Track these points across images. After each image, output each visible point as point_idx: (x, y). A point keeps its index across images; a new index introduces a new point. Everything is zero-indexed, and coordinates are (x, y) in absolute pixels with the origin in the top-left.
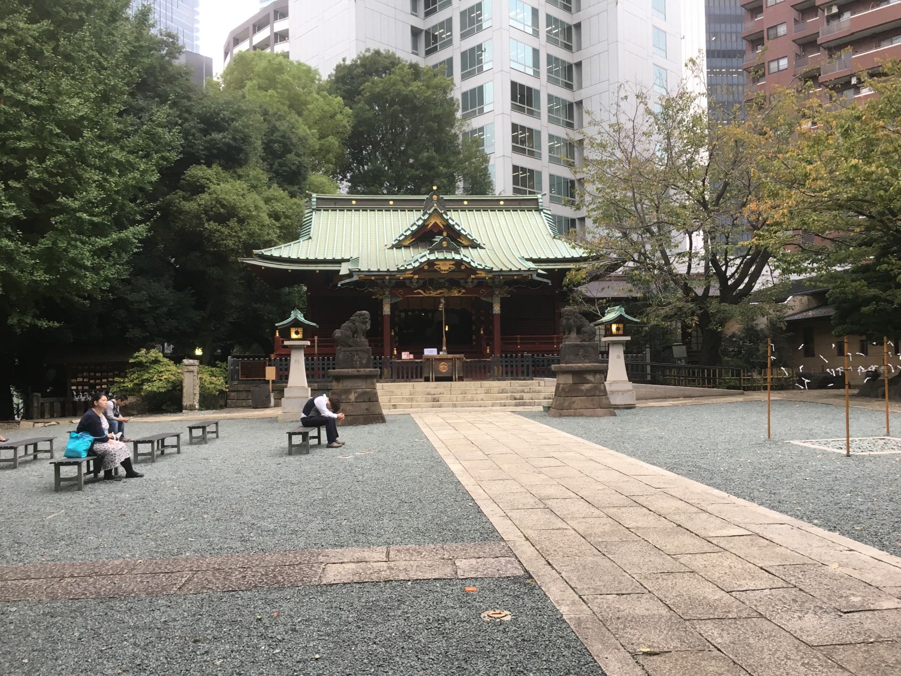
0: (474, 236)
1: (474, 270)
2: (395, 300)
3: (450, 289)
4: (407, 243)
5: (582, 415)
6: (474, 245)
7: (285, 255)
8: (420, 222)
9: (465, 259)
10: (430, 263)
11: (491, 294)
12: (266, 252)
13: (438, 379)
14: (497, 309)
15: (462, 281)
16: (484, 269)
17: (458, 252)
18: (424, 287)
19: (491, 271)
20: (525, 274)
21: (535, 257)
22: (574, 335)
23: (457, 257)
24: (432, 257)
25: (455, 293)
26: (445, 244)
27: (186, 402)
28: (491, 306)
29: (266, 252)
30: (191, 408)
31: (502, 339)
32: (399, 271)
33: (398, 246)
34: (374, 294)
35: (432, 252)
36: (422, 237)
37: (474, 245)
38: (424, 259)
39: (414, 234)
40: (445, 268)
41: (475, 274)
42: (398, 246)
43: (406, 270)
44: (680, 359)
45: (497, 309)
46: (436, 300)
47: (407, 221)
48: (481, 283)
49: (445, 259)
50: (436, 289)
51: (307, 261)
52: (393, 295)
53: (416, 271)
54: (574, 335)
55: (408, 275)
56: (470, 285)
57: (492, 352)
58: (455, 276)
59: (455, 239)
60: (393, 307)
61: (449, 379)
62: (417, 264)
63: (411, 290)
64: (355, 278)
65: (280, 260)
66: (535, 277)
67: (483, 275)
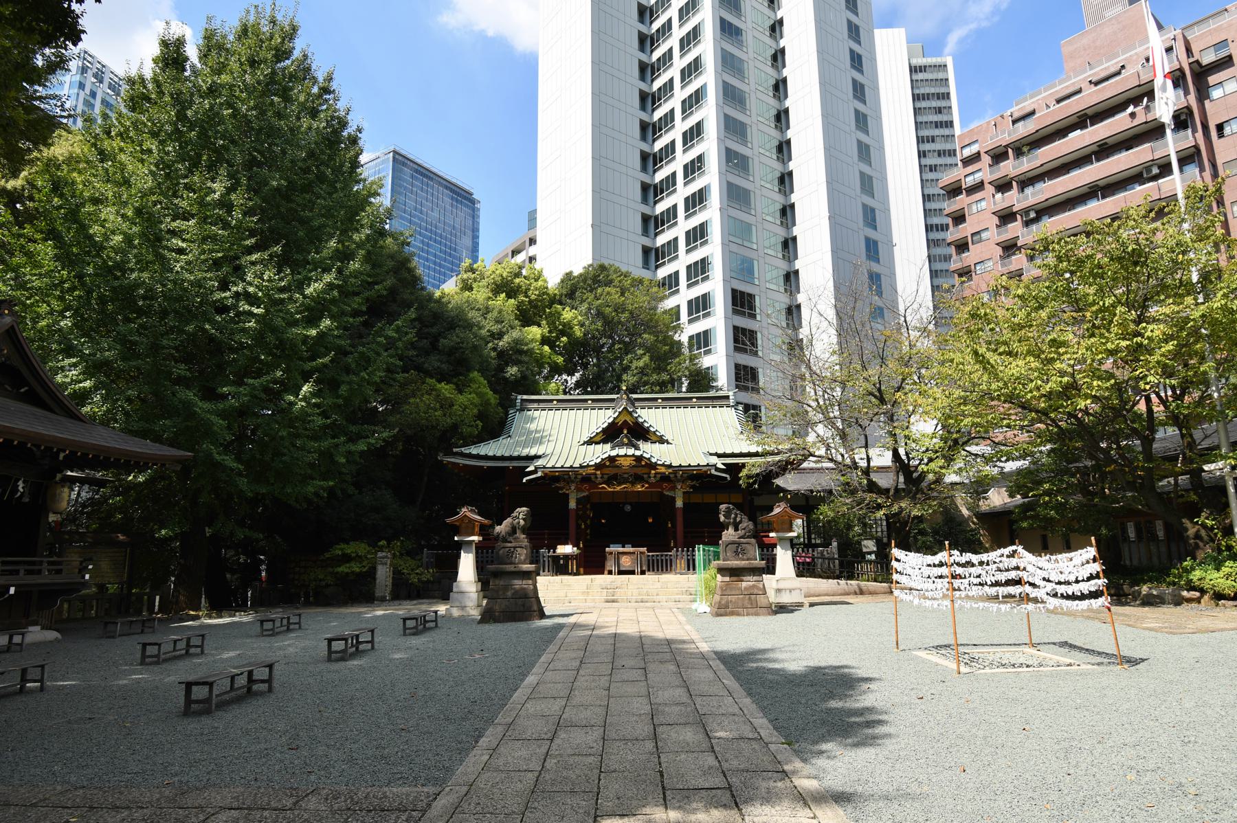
0: (661, 432)
1: (653, 466)
3: (633, 484)
5: (738, 614)
6: (662, 440)
7: (482, 453)
8: (611, 420)
10: (612, 459)
11: (674, 488)
12: (466, 450)
13: (621, 573)
16: (663, 465)
17: (637, 448)
18: (608, 483)
19: (670, 466)
20: (705, 469)
21: (720, 452)
22: (731, 530)
23: (638, 453)
24: (614, 453)
25: (639, 488)
27: (378, 594)
28: (673, 499)
29: (466, 450)
30: (383, 600)
32: (581, 467)
33: (590, 442)
34: (562, 488)
35: (613, 448)
36: (610, 434)
37: (662, 440)
39: (604, 431)
40: (626, 463)
42: (590, 442)
44: (870, 553)
45: (679, 503)
47: (601, 418)
48: (664, 478)
49: (626, 455)
50: (619, 484)
51: (503, 458)
52: (578, 490)
53: (598, 466)
54: (731, 530)
55: (590, 471)
56: (653, 480)
58: (640, 471)
59: (640, 433)
60: (578, 501)
61: (632, 572)
62: (598, 461)
63: (595, 485)
64: (539, 474)
65: (478, 457)
66: (713, 472)
67: (663, 470)
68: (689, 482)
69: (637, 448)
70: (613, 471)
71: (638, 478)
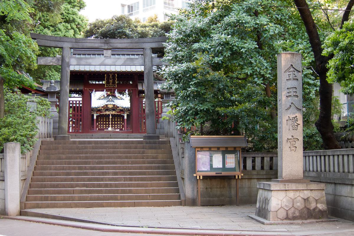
1: (118, 107)
2: (97, 115)
4: (102, 98)
9: (116, 104)
10: (107, 105)
11: (124, 113)
14: (126, 117)
15: (116, 110)
17: (114, 102)
19: (123, 107)
23: (114, 103)
24: (107, 103)
25: (114, 113)
26: (110, 100)
28: (124, 116)
31: (127, 126)
32: (98, 107)
35: (107, 102)
38: (105, 104)
41: (118, 108)
42: (99, 99)
43: (100, 107)
45: (126, 117)
46: (109, 115)
50: (109, 112)
53: (102, 107)
57: (124, 129)
62: (103, 105)
68: (128, 112)
69: (114, 102)
70: (107, 108)
71: (114, 110)
